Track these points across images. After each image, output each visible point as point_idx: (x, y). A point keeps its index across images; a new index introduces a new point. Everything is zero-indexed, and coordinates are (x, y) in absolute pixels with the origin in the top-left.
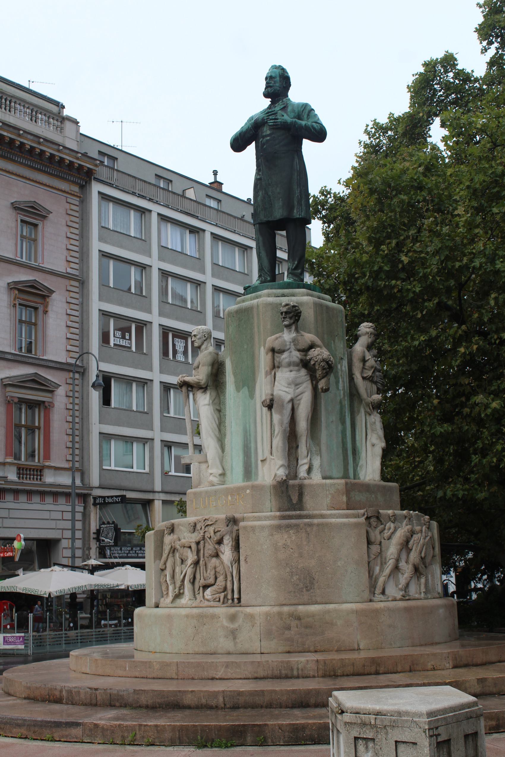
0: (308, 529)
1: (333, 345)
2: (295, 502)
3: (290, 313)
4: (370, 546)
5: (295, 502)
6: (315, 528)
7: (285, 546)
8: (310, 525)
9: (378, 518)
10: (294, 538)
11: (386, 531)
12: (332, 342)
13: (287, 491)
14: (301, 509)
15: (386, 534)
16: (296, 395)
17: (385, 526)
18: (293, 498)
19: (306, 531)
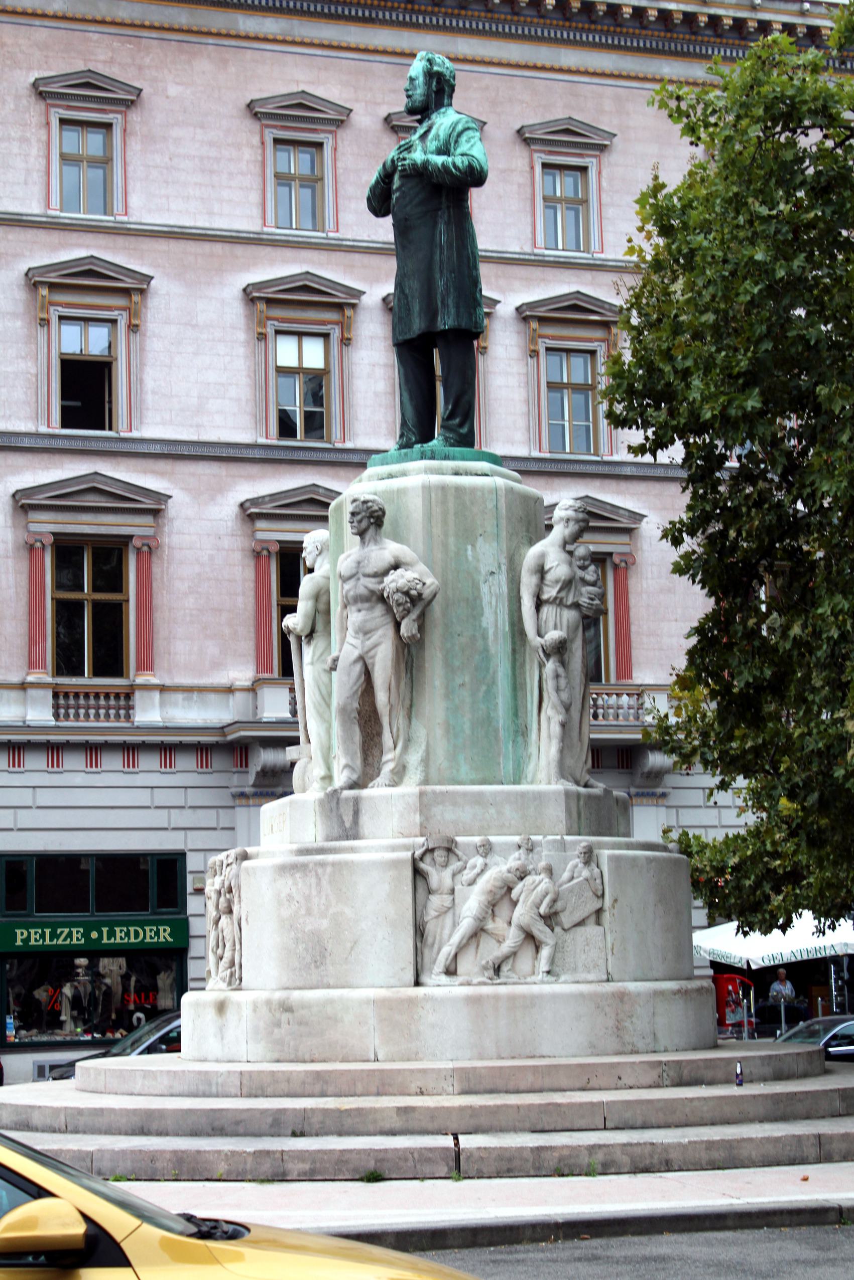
0: (320, 871)
1: (469, 553)
2: (348, 825)
3: (358, 513)
4: (431, 897)
5: (348, 825)
6: (329, 869)
7: (290, 898)
8: (322, 864)
9: (449, 850)
10: (300, 885)
11: (465, 872)
12: (469, 547)
13: (338, 808)
14: (356, 837)
15: (468, 875)
16: (366, 649)
17: (466, 863)
18: (345, 818)
19: (317, 875)
